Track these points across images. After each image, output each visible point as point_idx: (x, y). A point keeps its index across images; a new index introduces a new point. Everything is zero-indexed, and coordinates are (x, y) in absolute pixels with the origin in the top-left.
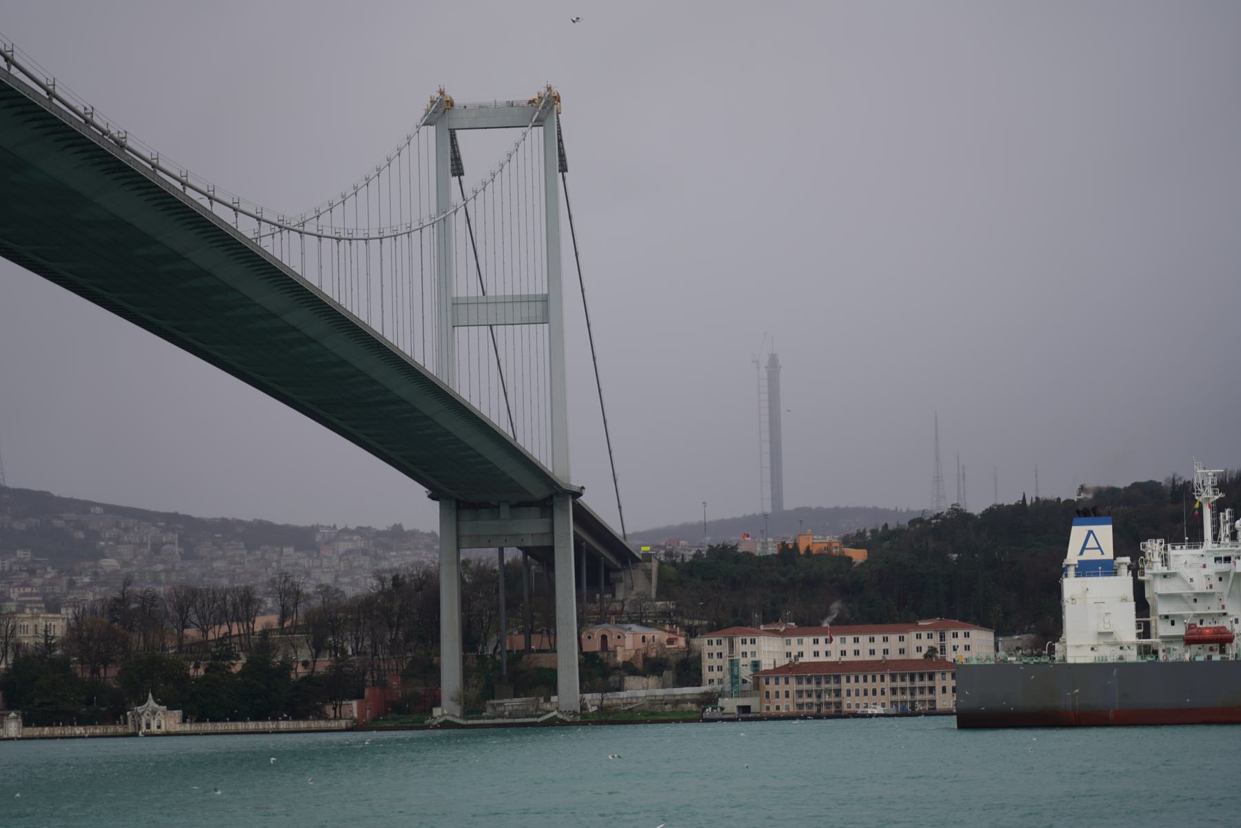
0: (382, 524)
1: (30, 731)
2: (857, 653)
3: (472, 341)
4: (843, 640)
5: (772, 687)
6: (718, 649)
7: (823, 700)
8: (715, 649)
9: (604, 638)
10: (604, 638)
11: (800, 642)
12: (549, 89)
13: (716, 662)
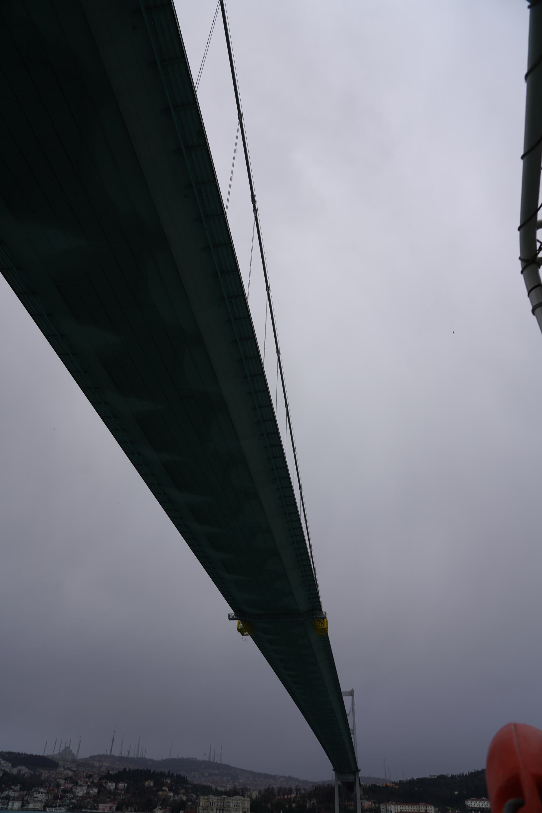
0: (287, 775)
4: (406, 807)
8: (383, 807)
11: (397, 807)
12: (352, 689)
13: (383, 810)
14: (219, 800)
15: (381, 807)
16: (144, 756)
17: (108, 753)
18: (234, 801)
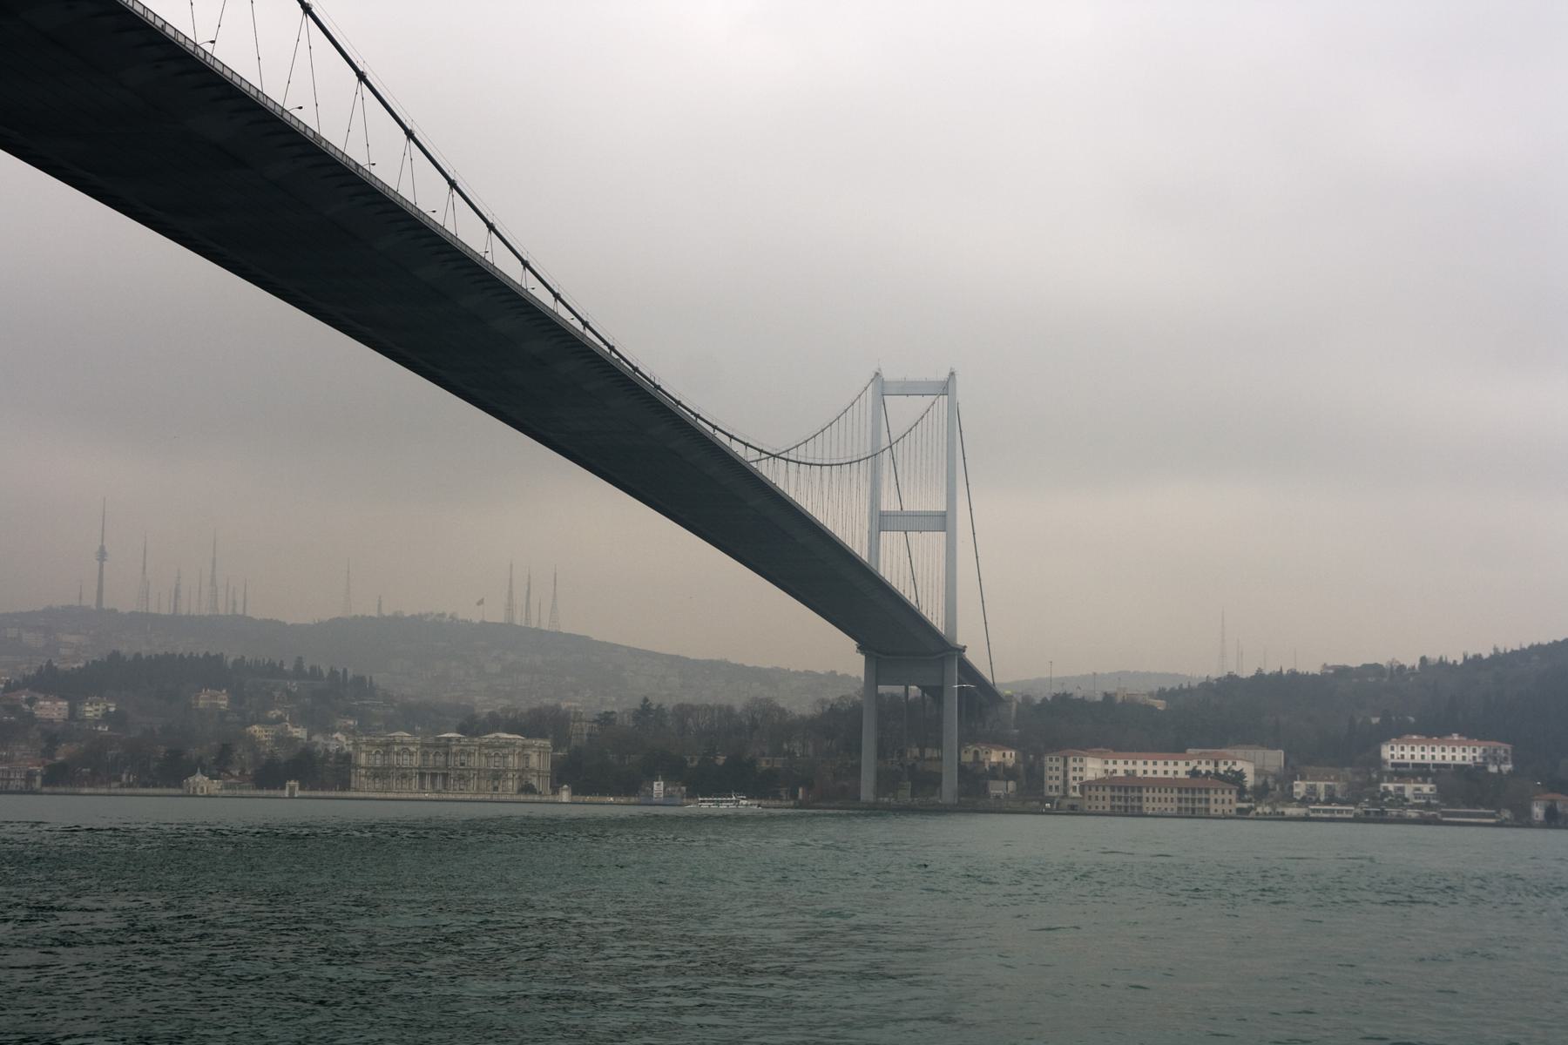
1: (577, 798)
2: (1155, 772)
3: (891, 541)
5: (1093, 793)
6: (1057, 764)
7: (1129, 804)
8: (1055, 764)
9: (976, 753)
10: (976, 753)
14: (428, 745)
15: (1048, 764)
16: (239, 611)
17: (90, 601)
18: (486, 751)
